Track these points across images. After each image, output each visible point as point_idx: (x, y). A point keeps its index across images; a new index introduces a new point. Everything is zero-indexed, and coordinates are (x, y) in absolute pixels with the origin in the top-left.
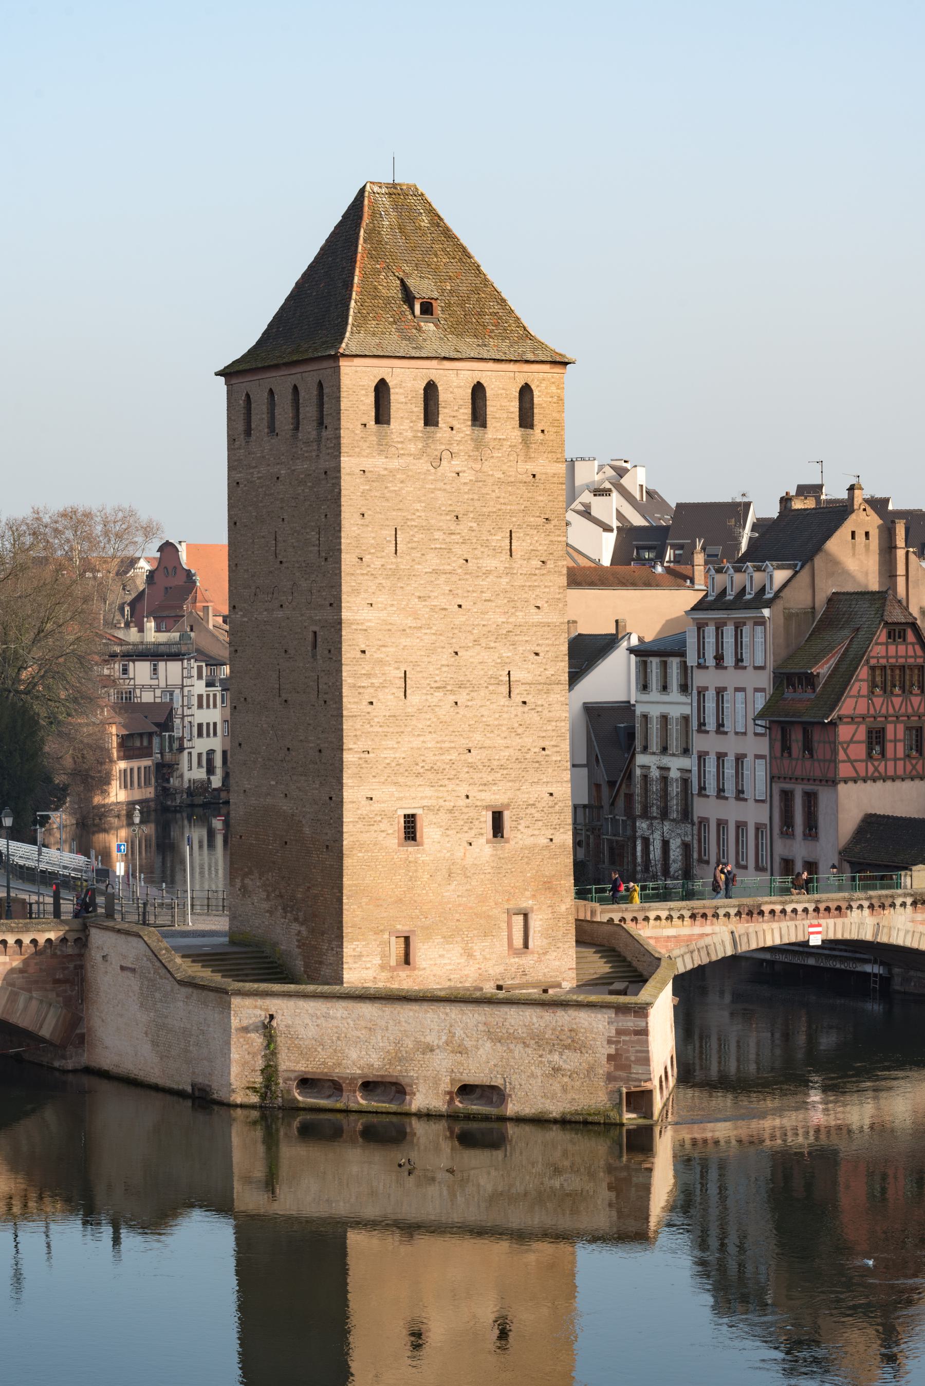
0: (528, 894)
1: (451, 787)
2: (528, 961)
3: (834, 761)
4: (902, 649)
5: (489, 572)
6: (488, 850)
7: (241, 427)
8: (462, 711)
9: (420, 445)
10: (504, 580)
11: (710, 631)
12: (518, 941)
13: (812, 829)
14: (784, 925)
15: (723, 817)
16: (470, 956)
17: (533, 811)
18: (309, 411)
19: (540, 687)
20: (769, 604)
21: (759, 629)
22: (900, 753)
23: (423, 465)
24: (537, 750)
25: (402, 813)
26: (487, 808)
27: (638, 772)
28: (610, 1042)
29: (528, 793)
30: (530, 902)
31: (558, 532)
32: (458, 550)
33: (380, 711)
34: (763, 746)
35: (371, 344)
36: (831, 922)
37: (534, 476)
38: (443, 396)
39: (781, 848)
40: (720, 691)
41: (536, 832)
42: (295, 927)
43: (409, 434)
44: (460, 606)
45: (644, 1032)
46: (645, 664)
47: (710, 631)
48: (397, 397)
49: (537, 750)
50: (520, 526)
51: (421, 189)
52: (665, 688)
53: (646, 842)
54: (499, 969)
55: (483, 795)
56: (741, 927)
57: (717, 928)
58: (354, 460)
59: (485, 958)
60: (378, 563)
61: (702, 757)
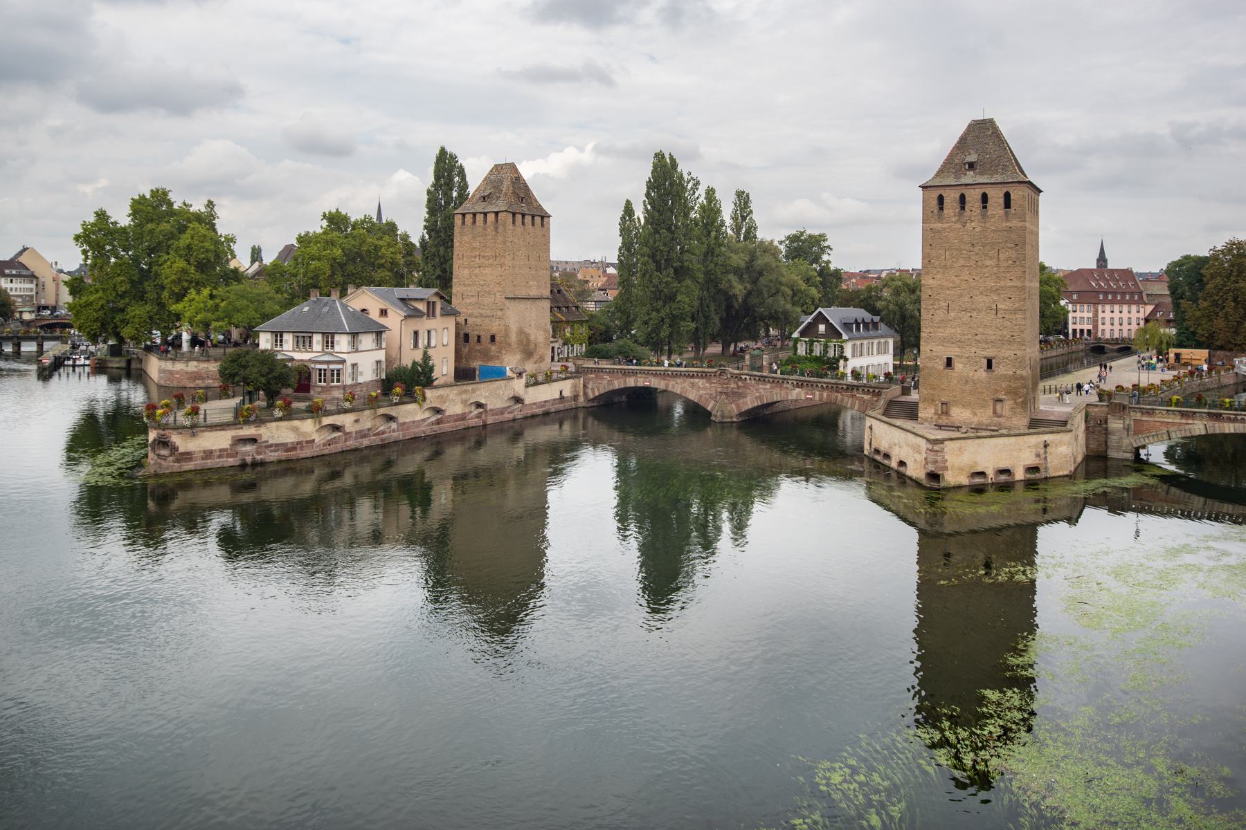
2: (1002, 420)
6: (984, 374)
14: (1237, 425)
16: (975, 414)
25: (945, 357)
54: (989, 421)
56: (1210, 424)
57: (1196, 422)
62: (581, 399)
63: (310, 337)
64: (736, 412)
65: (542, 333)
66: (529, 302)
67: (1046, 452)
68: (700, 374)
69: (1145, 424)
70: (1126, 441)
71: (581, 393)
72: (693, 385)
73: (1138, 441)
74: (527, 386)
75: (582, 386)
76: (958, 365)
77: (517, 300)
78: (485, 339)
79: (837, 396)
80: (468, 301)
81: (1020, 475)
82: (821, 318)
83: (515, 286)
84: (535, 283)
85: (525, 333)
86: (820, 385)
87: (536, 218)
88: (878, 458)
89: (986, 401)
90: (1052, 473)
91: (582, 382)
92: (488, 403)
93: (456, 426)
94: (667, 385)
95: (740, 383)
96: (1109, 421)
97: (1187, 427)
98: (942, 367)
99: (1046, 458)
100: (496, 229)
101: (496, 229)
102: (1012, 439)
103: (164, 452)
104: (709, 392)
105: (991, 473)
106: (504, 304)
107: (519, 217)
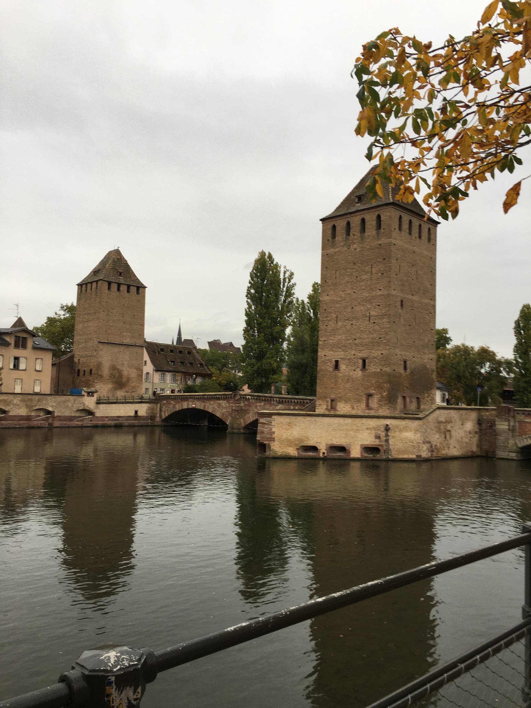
0: (373, 388)
1: (349, 351)
5: (363, 280)
6: (360, 372)
8: (354, 327)
9: (344, 243)
10: (369, 282)
16: (353, 408)
17: (375, 360)
19: (380, 317)
23: (345, 249)
24: (378, 339)
25: (334, 360)
26: (360, 358)
29: (374, 353)
30: (373, 391)
31: (388, 263)
32: (354, 274)
33: (329, 328)
37: (380, 245)
38: (352, 225)
41: (376, 367)
43: (341, 240)
44: (354, 292)
48: (338, 229)
49: (378, 339)
50: (375, 263)
55: (359, 354)
58: (325, 251)
59: (358, 410)
60: (331, 281)
62: (158, 419)
64: (243, 425)
65: (135, 370)
66: (122, 348)
67: (387, 435)
69: (528, 425)
70: (511, 442)
71: (158, 415)
73: (522, 441)
74: (98, 402)
75: (159, 410)
76: (342, 367)
77: (110, 345)
78: (87, 373)
80: (81, 346)
81: (356, 452)
83: (108, 334)
84: (129, 334)
85: (117, 369)
86: (293, 401)
87: (131, 287)
89: (362, 396)
90: (395, 455)
91: (159, 406)
92: (56, 411)
93: (19, 424)
94: (205, 406)
95: (246, 403)
96: (497, 423)
98: (331, 369)
99: (387, 441)
100: (96, 293)
101: (96, 293)
102: (349, 421)
105: (323, 449)
106: (98, 347)
107: (114, 287)
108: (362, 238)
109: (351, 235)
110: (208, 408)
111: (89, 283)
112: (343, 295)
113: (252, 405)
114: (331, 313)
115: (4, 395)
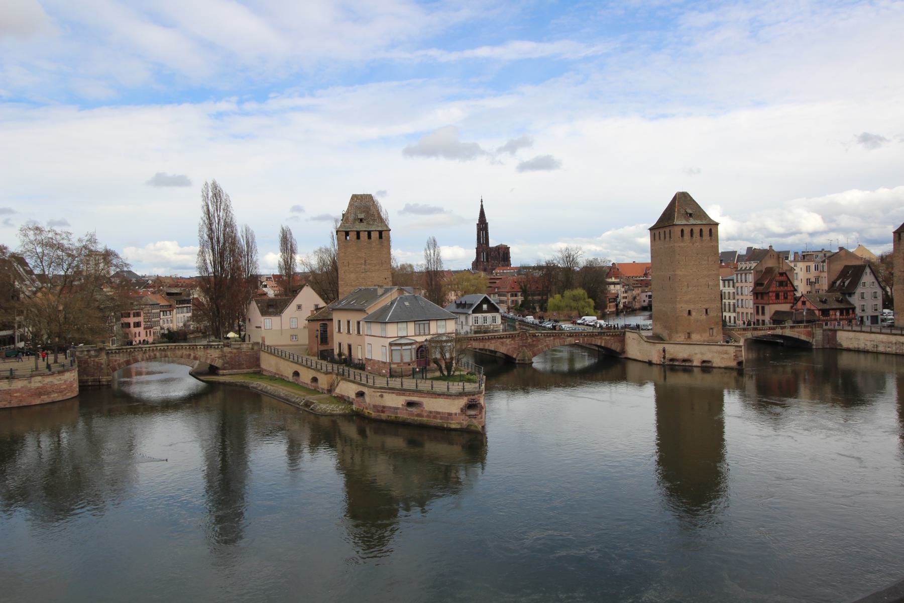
2: (714, 338)
3: (769, 300)
4: (783, 278)
7: (653, 239)
10: (707, 266)
11: (739, 276)
12: (711, 334)
13: (763, 313)
14: (762, 332)
15: (743, 311)
16: (701, 336)
18: (667, 235)
20: (752, 270)
21: (750, 275)
22: (783, 298)
23: (691, 244)
27: (723, 303)
28: (734, 353)
34: (752, 297)
35: (679, 223)
36: (772, 331)
39: (757, 317)
40: (742, 287)
42: (667, 331)
45: (741, 351)
46: (724, 282)
47: (739, 276)
48: (685, 232)
51: (688, 192)
52: (729, 286)
53: (725, 316)
57: (749, 332)
61: (738, 300)
63: (429, 324)
68: (508, 336)
72: (502, 343)
76: (693, 313)
79: (592, 340)
82: (486, 300)
86: (583, 334)
88: (677, 363)
94: (484, 346)
95: (534, 339)
97: (745, 335)
103: (472, 412)
104: (513, 346)
108: (702, 240)
109: (694, 236)
110: (489, 346)
111: (365, 231)
112: (691, 271)
113: (541, 340)
114: (683, 282)
115: (851, 352)
